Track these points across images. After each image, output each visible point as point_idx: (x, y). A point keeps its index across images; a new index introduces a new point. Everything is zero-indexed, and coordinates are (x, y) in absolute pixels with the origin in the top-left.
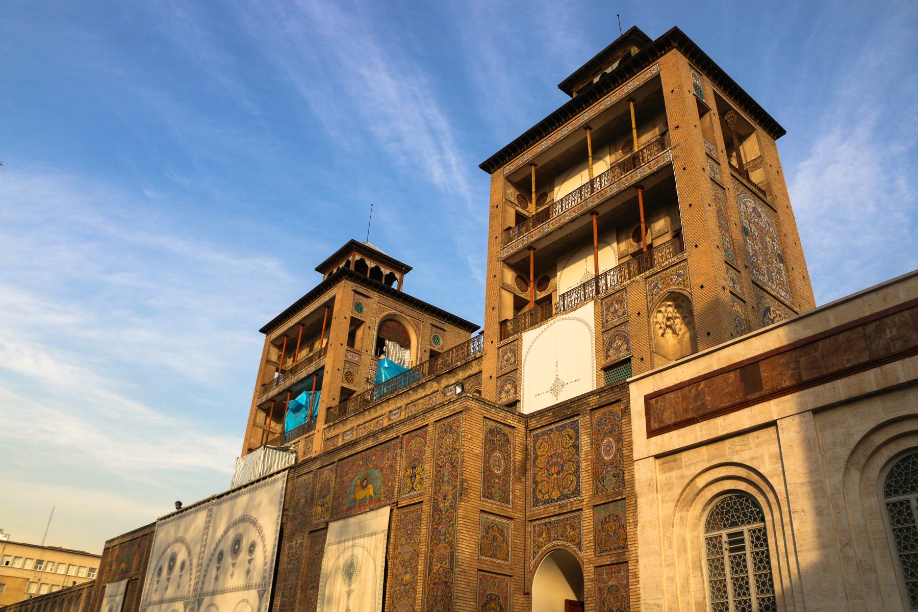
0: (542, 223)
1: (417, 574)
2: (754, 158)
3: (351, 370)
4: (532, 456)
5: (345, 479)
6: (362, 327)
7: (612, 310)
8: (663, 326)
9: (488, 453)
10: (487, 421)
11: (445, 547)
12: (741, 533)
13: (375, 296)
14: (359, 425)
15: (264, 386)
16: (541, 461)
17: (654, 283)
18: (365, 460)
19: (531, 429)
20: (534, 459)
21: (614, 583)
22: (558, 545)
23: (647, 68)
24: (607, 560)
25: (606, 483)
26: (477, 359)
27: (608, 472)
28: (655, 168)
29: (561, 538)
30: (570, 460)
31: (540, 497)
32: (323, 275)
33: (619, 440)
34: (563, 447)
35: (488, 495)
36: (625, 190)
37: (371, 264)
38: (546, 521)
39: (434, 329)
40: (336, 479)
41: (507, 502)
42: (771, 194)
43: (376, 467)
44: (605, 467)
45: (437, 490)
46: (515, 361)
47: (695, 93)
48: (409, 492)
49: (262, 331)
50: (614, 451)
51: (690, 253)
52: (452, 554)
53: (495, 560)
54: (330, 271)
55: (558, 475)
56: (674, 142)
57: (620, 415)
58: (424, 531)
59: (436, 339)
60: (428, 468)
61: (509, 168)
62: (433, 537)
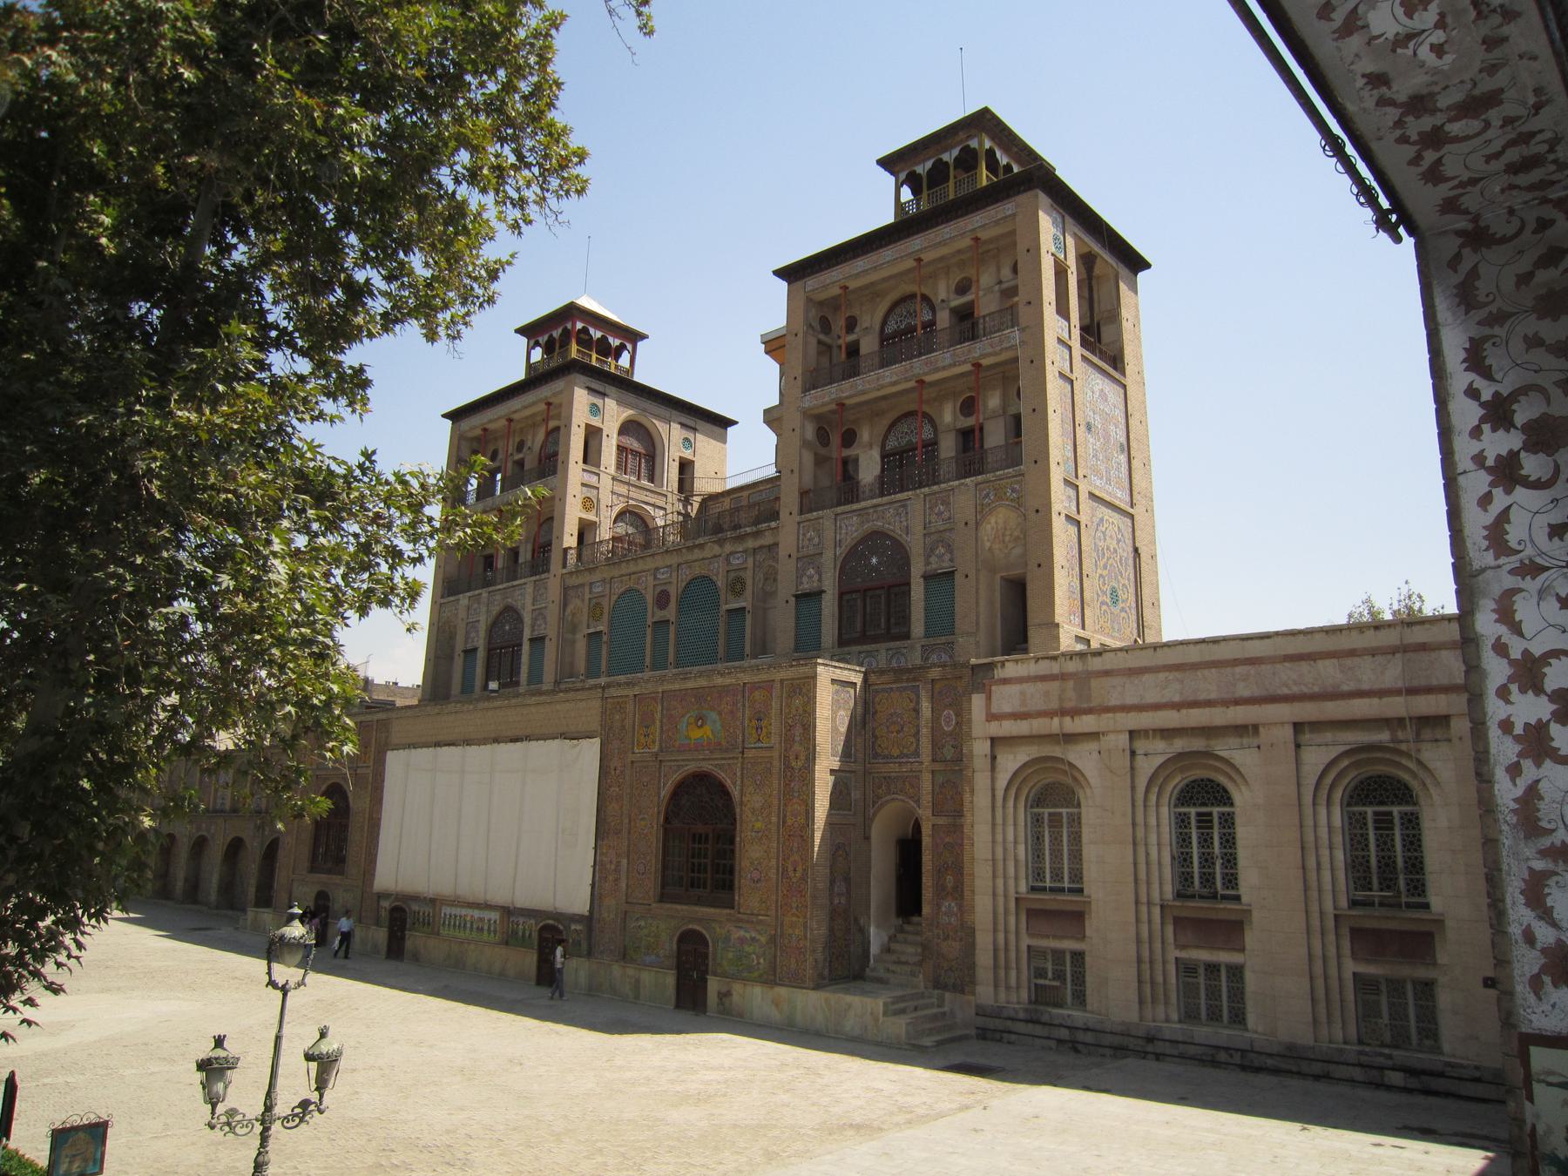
9: (834, 712)
24: (941, 821)
25: (945, 750)
31: (879, 751)
37: (596, 334)
41: (850, 756)
42: (1123, 362)
49: (445, 416)
52: (807, 812)
56: (1023, 321)
58: (775, 784)
61: (812, 283)
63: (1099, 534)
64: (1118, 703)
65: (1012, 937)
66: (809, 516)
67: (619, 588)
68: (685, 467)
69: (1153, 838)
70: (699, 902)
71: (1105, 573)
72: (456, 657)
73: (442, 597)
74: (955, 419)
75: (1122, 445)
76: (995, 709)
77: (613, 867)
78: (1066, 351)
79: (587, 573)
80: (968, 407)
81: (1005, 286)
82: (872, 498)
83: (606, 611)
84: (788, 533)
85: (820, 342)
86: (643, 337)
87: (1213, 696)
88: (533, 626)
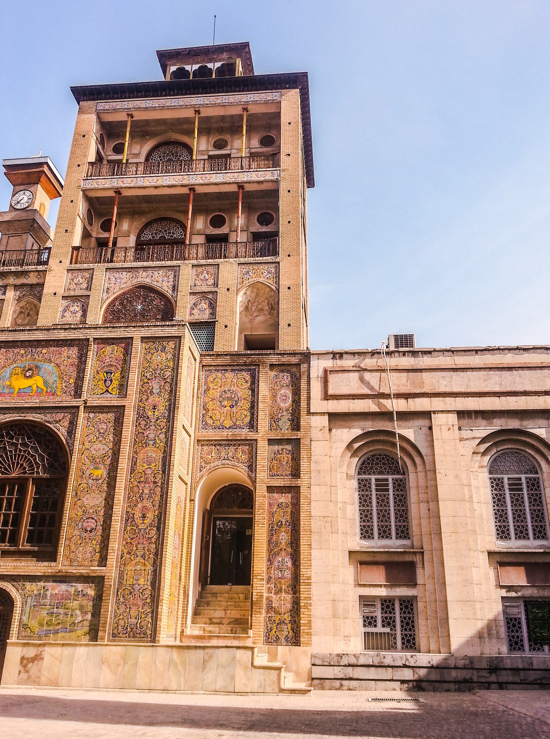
4: (204, 388)
7: (202, 277)
11: (153, 451)
12: (387, 480)
17: (246, 270)
19: (205, 364)
20: (205, 390)
21: (284, 501)
25: (280, 423)
26: (37, 271)
27: (283, 416)
28: (262, 179)
29: (231, 459)
30: (244, 399)
31: (210, 421)
36: (230, 183)
43: (50, 361)
44: (281, 411)
45: (144, 399)
48: (103, 394)
55: (231, 408)
62: (137, 440)
64: (448, 390)
66: (78, 266)
74: (206, 227)
80: (217, 222)
81: (253, 150)
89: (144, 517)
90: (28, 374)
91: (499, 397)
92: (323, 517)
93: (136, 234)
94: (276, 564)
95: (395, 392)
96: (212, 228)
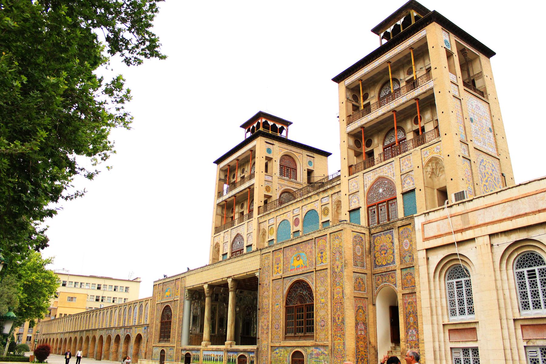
0: (367, 114)
1: (328, 299)
2: (478, 73)
3: (268, 185)
4: (373, 245)
5: (288, 256)
6: (272, 161)
7: (405, 164)
8: (430, 173)
9: (354, 246)
10: (353, 232)
13: (277, 143)
14: (277, 216)
15: (220, 194)
16: (377, 248)
17: (425, 152)
18: (297, 248)
22: (386, 284)
23: (419, 32)
24: (407, 291)
25: (406, 259)
26: (338, 185)
28: (424, 90)
31: (377, 263)
32: (244, 129)
33: (411, 241)
34: (387, 242)
35: (356, 265)
36: (410, 100)
37: (271, 123)
38: (380, 274)
39: (309, 157)
40: (283, 256)
41: (363, 266)
42: (486, 93)
46: (358, 187)
47: (445, 46)
49: (215, 162)
50: (409, 245)
51: (443, 138)
52: (343, 291)
53: (360, 292)
54: (249, 127)
57: (411, 230)
58: (329, 281)
59: (310, 163)
60: (327, 254)
63: (481, 166)
65: (442, 344)
67: (279, 220)
68: (310, 172)
69: (506, 286)
70: (300, 338)
71: (487, 184)
72: (220, 257)
73: (215, 234)
74: (412, 126)
75: (490, 129)
76: (427, 236)
77: (266, 327)
78: (456, 87)
79: (267, 215)
81: (427, 67)
82: (378, 164)
83: (275, 230)
84: (345, 186)
85: (353, 105)
86: (291, 123)
87: (527, 211)
88: (247, 241)
89: (339, 319)
90: (298, 259)
91: (511, 220)
92: (427, 308)
93: (382, 143)
94: (409, 333)
95: (455, 230)
96: (415, 125)
